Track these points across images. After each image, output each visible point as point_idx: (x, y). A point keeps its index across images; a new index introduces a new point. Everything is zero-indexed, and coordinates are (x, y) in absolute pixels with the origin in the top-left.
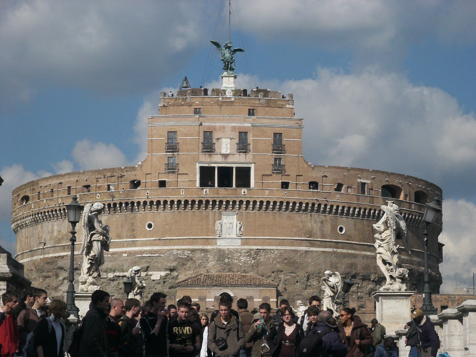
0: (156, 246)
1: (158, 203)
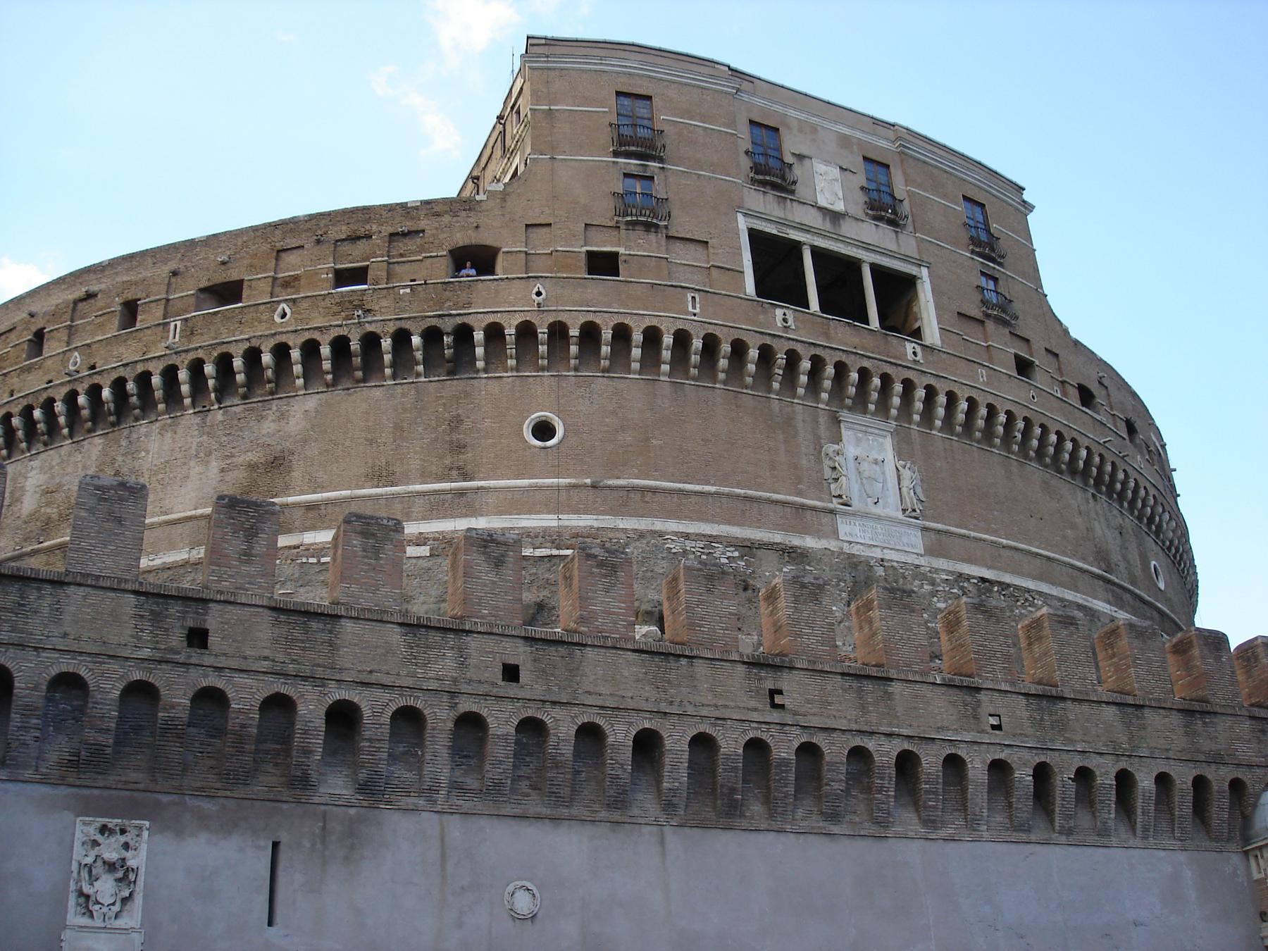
0: (577, 512)
1: (590, 333)
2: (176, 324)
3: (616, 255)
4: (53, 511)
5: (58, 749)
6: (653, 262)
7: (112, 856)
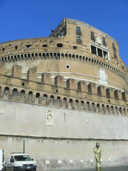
2: (23, 50)
3: (76, 46)
4: (6, 71)
5: (44, 102)
6: (81, 48)
7: (50, 114)
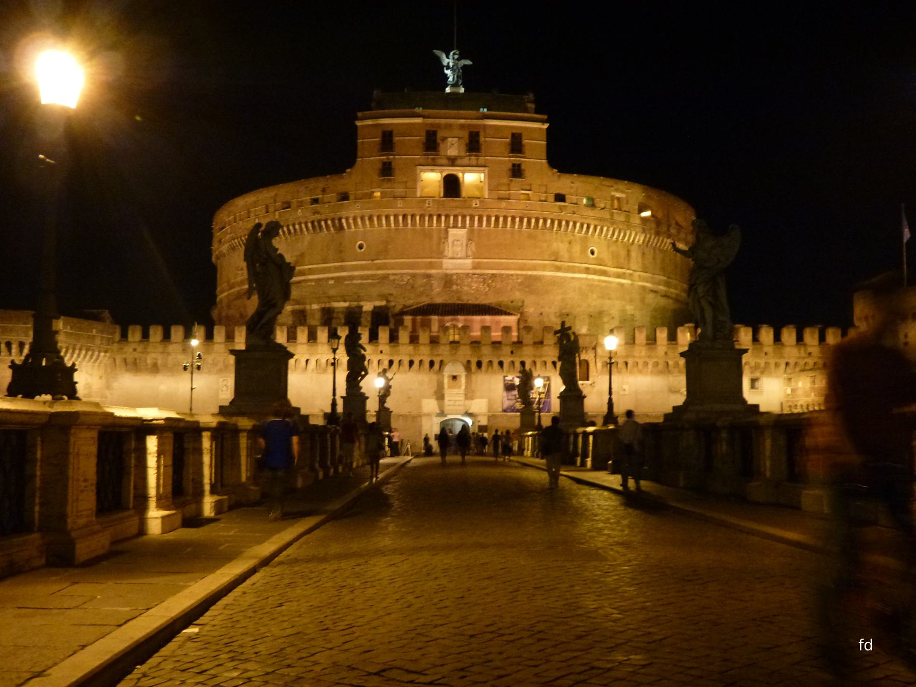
0: (369, 270)
